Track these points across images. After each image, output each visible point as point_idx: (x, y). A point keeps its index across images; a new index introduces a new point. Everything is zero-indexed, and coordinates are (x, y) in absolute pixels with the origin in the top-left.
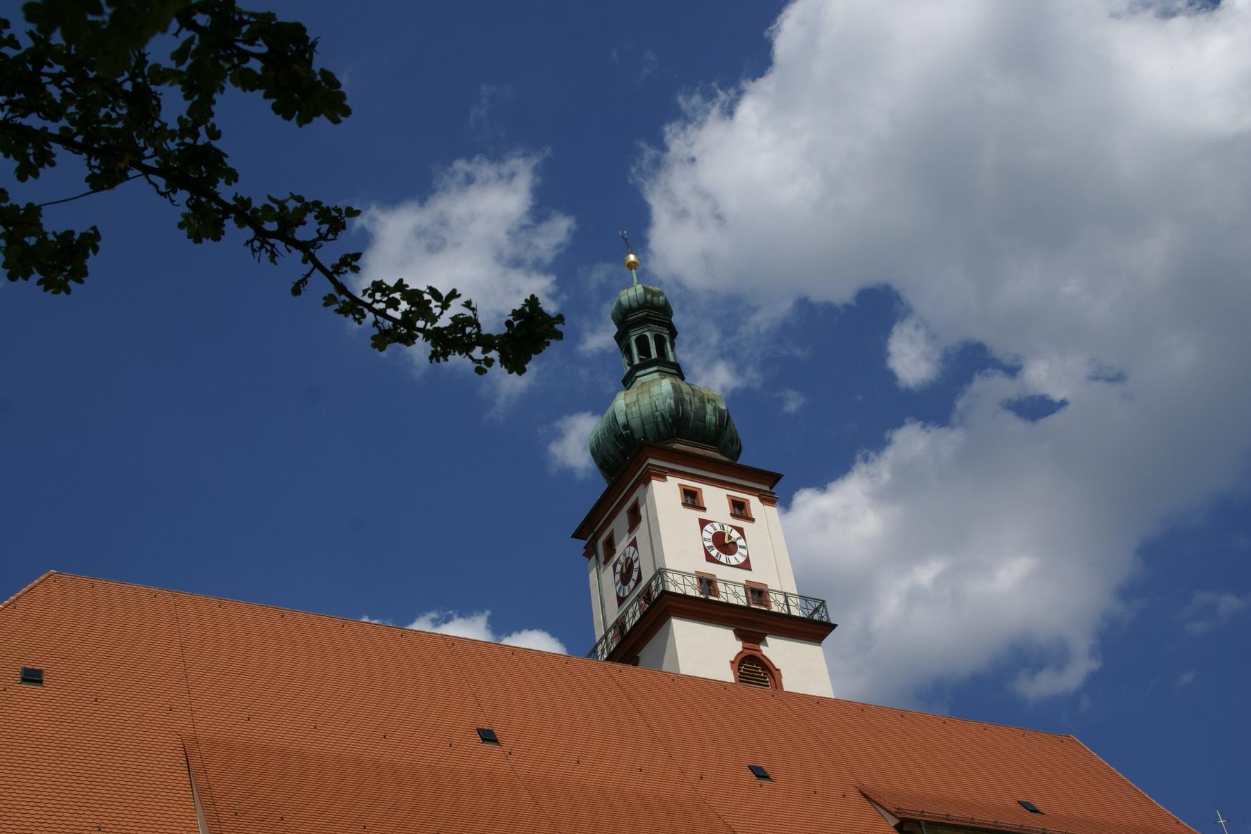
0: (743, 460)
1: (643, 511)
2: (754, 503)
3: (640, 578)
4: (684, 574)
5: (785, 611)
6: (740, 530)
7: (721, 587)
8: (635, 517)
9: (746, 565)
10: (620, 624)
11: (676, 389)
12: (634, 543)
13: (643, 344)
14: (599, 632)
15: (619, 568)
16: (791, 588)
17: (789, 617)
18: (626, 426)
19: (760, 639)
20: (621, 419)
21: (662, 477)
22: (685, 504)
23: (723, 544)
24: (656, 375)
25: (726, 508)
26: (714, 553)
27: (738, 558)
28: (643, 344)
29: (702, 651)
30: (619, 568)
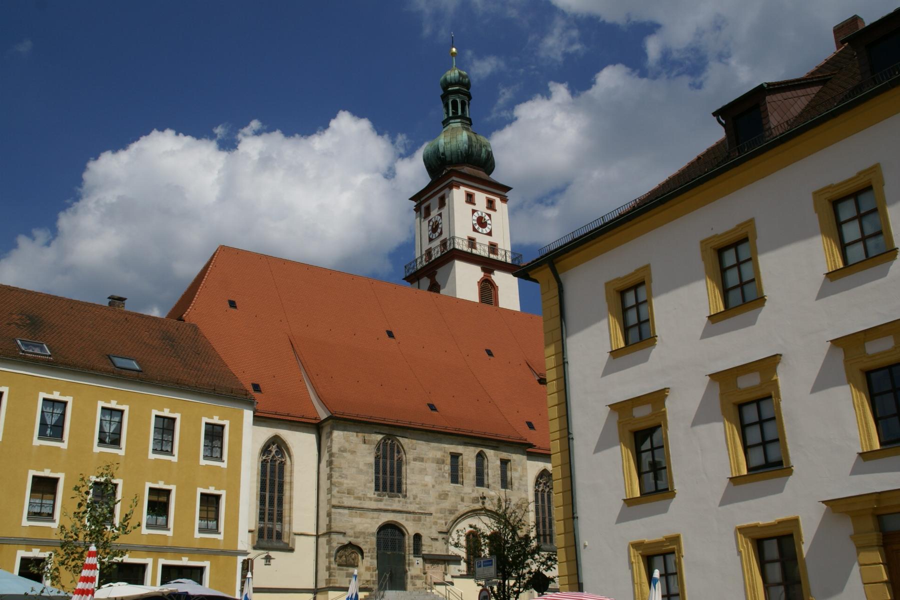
0: (495, 176)
1: (447, 201)
2: (497, 201)
3: (441, 234)
4: (463, 240)
5: (503, 260)
6: (489, 215)
7: (478, 246)
8: (442, 203)
10: (429, 253)
11: (470, 138)
12: (440, 215)
13: (455, 104)
14: (418, 255)
16: (509, 248)
17: (505, 263)
18: (443, 154)
19: (491, 272)
20: (441, 150)
21: (458, 187)
22: (467, 202)
23: (482, 222)
24: (459, 125)
26: (477, 227)
28: (455, 104)
29: (465, 281)
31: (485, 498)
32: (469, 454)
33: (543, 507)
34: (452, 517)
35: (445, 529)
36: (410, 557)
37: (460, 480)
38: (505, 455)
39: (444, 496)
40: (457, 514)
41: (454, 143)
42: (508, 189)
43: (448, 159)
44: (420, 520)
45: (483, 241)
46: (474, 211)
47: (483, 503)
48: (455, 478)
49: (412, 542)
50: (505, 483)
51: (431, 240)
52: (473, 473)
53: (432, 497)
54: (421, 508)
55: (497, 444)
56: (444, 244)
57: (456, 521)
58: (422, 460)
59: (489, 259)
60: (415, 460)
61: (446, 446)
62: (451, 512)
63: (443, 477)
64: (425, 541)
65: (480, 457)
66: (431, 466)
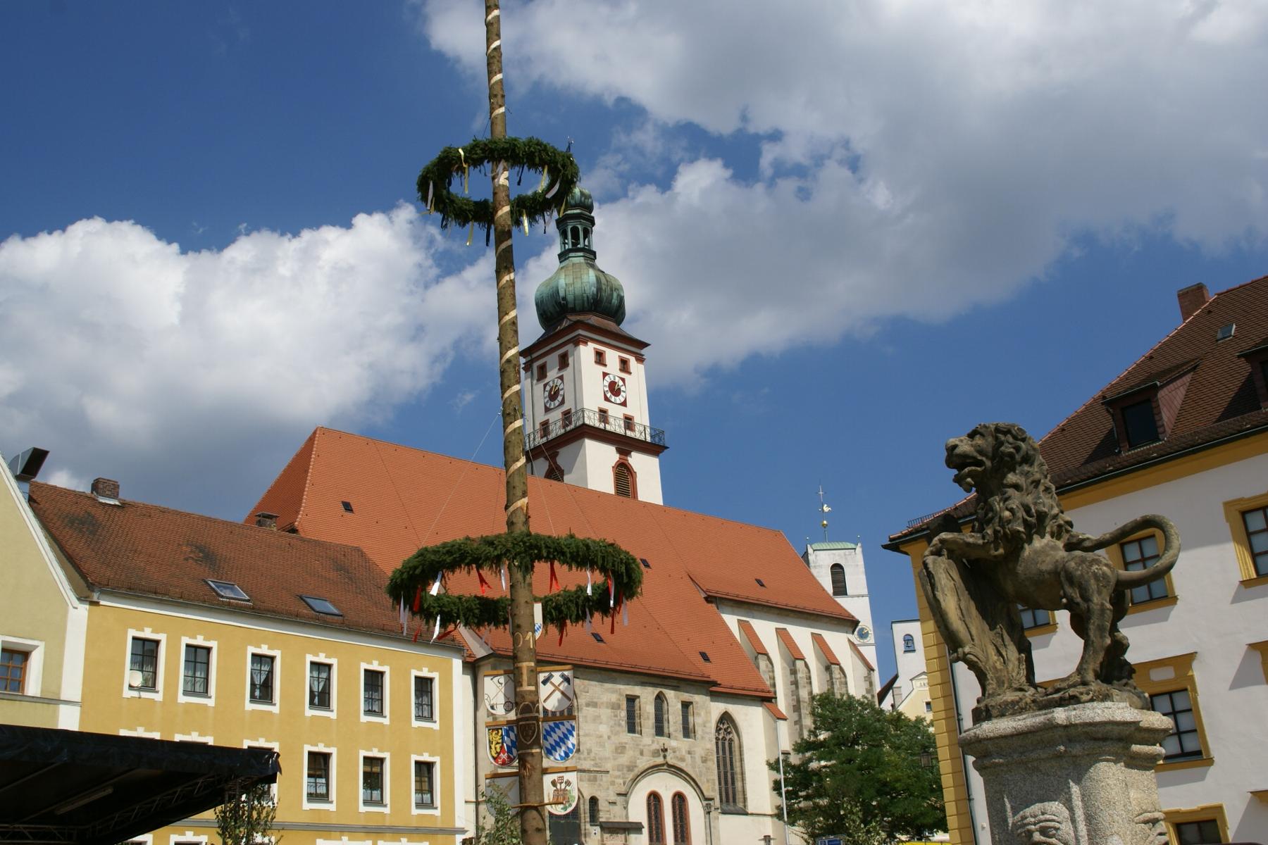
2: (632, 360)
3: (562, 402)
6: (623, 380)
7: (611, 420)
8: (564, 362)
9: (624, 404)
10: (545, 425)
12: (561, 378)
15: (548, 388)
17: (645, 442)
18: (564, 299)
19: (627, 453)
20: (562, 293)
21: (586, 343)
23: (614, 389)
24: (582, 260)
25: (617, 365)
26: (609, 395)
27: (620, 399)
30: (548, 388)
31: (665, 750)
32: (646, 696)
33: (724, 758)
34: (631, 776)
35: (623, 790)
36: (587, 826)
37: (638, 728)
38: (686, 696)
39: (621, 749)
40: (637, 771)
41: (578, 285)
42: (643, 345)
43: (570, 306)
44: (595, 779)
45: (616, 412)
46: (605, 375)
47: (665, 757)
48: (632, 728)
49: (587, 807)
50: (687, 731)
51: (547, 410)
52: (652, 721)
53: (608, 751)
54: (596, 765)
55: (710, 688)
56: (567, 415)
57: (635, 780)
58: (595, 705)
59: (625, 436)
60: (588, 705)
61: (622, 687)
62: (630, 769)
63: (620, 725)
64: (602, 805)
65: (660, 699)
66: (605, 713)
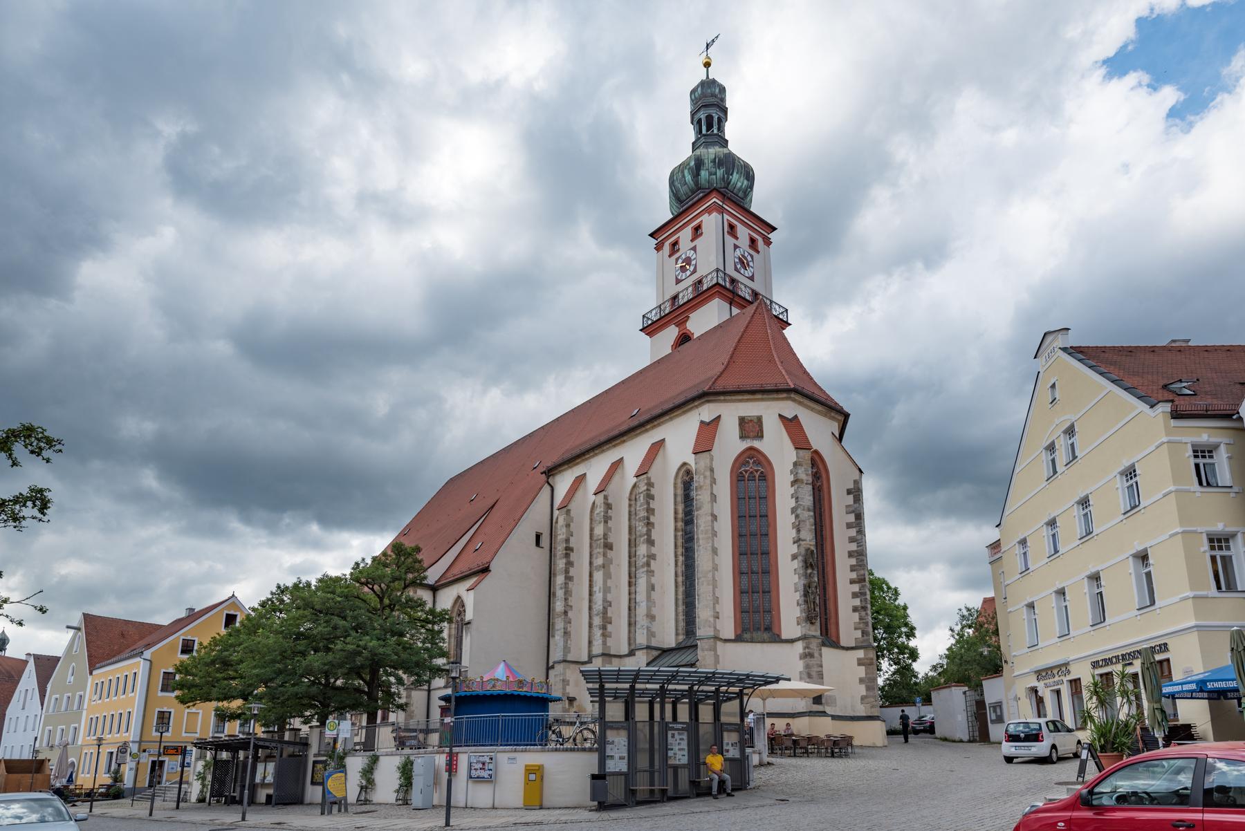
3: (695, 271)
9: (752, 278)
12: (694, 249)
23: (743, 262)
25: (747, 242)
27: (748, 273)
46: (736, 247)
51: (678, 281)
